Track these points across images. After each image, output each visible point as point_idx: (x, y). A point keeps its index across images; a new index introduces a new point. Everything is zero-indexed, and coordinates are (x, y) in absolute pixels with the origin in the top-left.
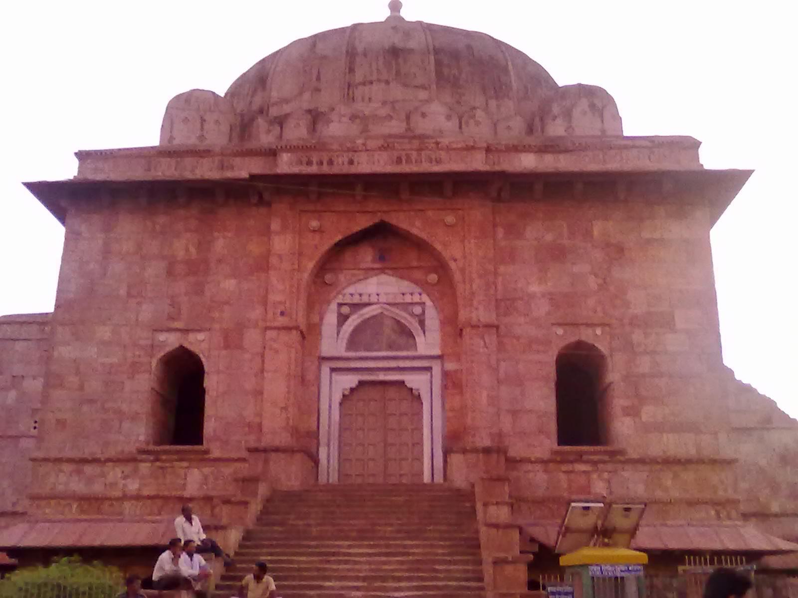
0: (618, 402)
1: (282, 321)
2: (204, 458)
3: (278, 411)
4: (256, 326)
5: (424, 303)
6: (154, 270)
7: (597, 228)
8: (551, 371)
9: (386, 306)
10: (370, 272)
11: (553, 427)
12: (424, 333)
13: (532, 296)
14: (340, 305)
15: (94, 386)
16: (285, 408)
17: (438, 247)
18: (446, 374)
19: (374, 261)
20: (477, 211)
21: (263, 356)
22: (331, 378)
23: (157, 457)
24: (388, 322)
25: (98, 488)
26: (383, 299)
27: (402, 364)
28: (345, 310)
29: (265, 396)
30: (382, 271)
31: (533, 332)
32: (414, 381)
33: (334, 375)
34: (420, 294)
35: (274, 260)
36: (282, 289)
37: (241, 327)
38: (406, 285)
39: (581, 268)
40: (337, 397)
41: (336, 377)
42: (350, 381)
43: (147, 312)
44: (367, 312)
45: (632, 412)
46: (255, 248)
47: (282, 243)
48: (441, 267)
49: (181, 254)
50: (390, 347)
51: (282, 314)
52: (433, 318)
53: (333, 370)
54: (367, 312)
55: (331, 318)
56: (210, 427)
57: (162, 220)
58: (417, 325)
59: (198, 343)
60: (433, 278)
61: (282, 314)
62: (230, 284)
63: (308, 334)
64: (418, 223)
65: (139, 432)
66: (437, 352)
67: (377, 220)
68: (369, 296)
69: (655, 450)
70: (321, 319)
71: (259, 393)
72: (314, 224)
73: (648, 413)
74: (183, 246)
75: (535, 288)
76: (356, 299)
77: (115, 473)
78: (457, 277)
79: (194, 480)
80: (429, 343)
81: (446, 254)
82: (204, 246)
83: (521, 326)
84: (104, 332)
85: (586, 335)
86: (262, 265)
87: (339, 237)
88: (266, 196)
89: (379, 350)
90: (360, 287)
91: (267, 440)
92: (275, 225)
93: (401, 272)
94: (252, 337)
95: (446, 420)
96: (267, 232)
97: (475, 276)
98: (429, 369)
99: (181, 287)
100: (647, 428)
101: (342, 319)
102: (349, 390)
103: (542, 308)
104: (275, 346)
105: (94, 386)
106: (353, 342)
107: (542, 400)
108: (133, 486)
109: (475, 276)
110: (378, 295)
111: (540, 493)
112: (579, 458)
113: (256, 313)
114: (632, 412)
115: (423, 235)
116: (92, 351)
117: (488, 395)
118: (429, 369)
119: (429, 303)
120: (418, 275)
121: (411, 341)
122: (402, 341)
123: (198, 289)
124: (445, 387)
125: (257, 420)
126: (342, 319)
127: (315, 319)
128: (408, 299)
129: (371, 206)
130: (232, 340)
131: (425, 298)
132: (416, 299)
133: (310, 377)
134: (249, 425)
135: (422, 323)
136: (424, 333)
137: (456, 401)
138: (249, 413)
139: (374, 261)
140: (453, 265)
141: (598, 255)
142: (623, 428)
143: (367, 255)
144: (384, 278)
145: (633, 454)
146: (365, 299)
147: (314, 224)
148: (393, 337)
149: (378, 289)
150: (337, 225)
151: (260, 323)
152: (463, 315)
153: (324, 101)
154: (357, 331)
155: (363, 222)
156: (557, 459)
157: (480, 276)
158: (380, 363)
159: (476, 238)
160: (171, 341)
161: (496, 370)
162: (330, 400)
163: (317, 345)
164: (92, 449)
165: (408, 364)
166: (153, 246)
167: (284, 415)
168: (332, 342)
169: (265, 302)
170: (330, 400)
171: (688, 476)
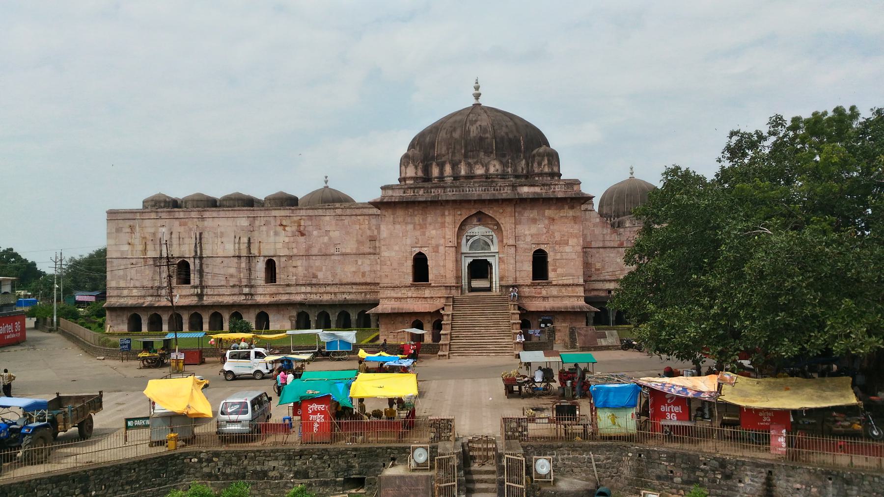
0: (550, 268)
1: (450, 244)
2: (429, 286)
6: (410, 227)
7: (548, 212)
8: (531, 258)
11: (531, 275)
13: (526, 235)
15: (395, 265)
18: (500, 258)
20: (509, 209)
23: (416, 286)
25: (399, 295)
31: (526, 246)
32: (490, 260)
36: (450, 233)
37: (437, 246)
38: (487, 229)
39: (541, 226)
42: (470, 260)
43: (409, 241)
44: (475, 238)
45: (555, 270)
46: (439, 220)
47: (449, 219)
48: (498, 224)
49: (417, 222)
52: (495, 240)
54: (475, 238)
55: (464, 241)
56: (430, 277)
57: (411, 210)
59: (424, 251)
60: (496, 227)
62: (434, 232)
65: (409, 279)
69: (561, 282)
71: (444, 266)
73: (559, 271)
74: (418, 219)
75: (527, 232)
77: (404, 291)
79: (427, 293)
80: (494, 248)
82: (424, 220)
83: (521, 244)
84: (396, 248)
85: (542, 247)
86: (443, 225)
90: (473, 230)
92: (447, 213)
93: (484, 225)
94: (441, 249)
96: (443, 215)
99: (418, 233)
100: (558, 276)
101: (468, 241)
103: (528, 239)
105: (395, 265)
106: (471, 247)
107: (528, 267)
108: (410, 295)
111: (527, 294)
112: (539, 284)
113: (442, 241)
114: (555, 270)
116: (393, 254)
123: (424, 234)
126: (468, 241)
129: (476, 206)
130: (436, 249)
137: (503, 266)
138: (442, 272)
141: (546, 222)
142: (551, 275)
145: (554, 283)
147: (459, 213)
149: (478, 231)
152: (505, 241)
153: (457, 157)
155: (474, 212)
156: (532, 285)
158: (480, 255)
160: (417, 250)
164: (397, 283)
166: (409, 219)
168: (465, 249)
169: (444, 238)
171: (570, 289)
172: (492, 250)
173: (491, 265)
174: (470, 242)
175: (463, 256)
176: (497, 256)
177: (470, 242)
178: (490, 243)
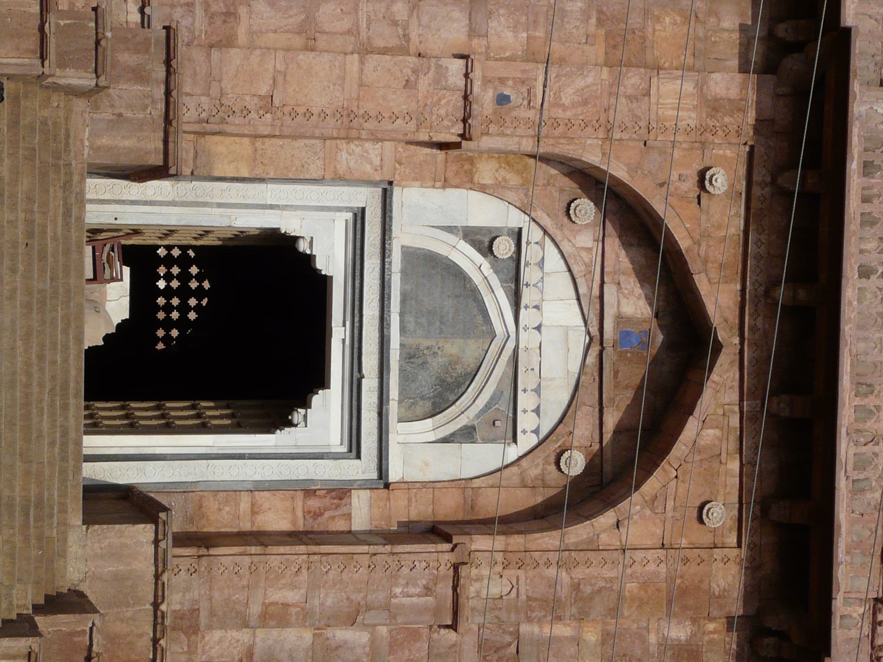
3: (264, 90)
4: (473, 32)
5: (515, 440)
9: (511, 345)
10: (594, 308)
12: (445, 440)
14: (518, 235)
16: (268, 103)
17: (652, 485)
18: (340, 492)
19: (619, 318)
21: (403, 50)
22: (339, 209)
24: (466, 350)
26: (528, 339)
27: (370, 385)
28: (504, 248)
29: (304, 58)
30: (596, 340)
33: (349, 216)
34: (536, 432)
35: (633, 80)
38: (557, 398)
40: (289, 224)
41: (341, 223)
42: (330, 257)
44: (497, 302)
47: (673, 98)
50: (409, 356)
51: (502, 100)
53: (360, 216)
54: (497, 302)
58: (463, 421)
61: (502, 100)
63: (452, 152)
64: (710, 434)
66: (395, 474)
67: (722, 336)
68: (537, 307)
70: (483, 189)
71: (310, 38)
72: (720, 182)
76: (529, 274)
78: (578, 533)
81: (634, 504)
87: (684, 243)
88: (792, 63)
89: (403, 330)
91: (193, 62)
95: (230, 492)
97: (579, 573)
98: (355, 449)
101: (483, 241)
102: (308, 252)
104: (424, 83)
106: (428, 265)
109: (579, 573)
110: (538, 328)
115: (679, 449)
117: (286, 605)
118: (355, 449)
119: (513, 452)
120: (584, 429)
121: (425, 406)
122: (425, 382)
124: (308, 490)
125: (242, 33)
126: (483, 241)
127: (486, 172)
128: (525, 401)
131: (527, 441)
132: (526, 421)
133: (349, 156)
134: (230, 15)
135: (467, 434)
136: (445, 440)
139: (619, 318)
140: (607, 518)
143: (632, 302)
144: (579, 340)
146: (528, 296)
148: (436, 364)
150: (713, 233)
151: (478, 44)
154: (455, 273)
155: (720, 299)
157: (576, 587)
159: (670, 579)
161: (351, 621)
162: (285, 207)
163: (419, 178)
165: (369, 399)
167: (251, 103)
170: (285, 207)
172: (398, 432)
173: (277, 420)
174: (466, 257)
175: (366, 197)
176: (363, 469)
177: (466, 257)
178: (468, 408)
